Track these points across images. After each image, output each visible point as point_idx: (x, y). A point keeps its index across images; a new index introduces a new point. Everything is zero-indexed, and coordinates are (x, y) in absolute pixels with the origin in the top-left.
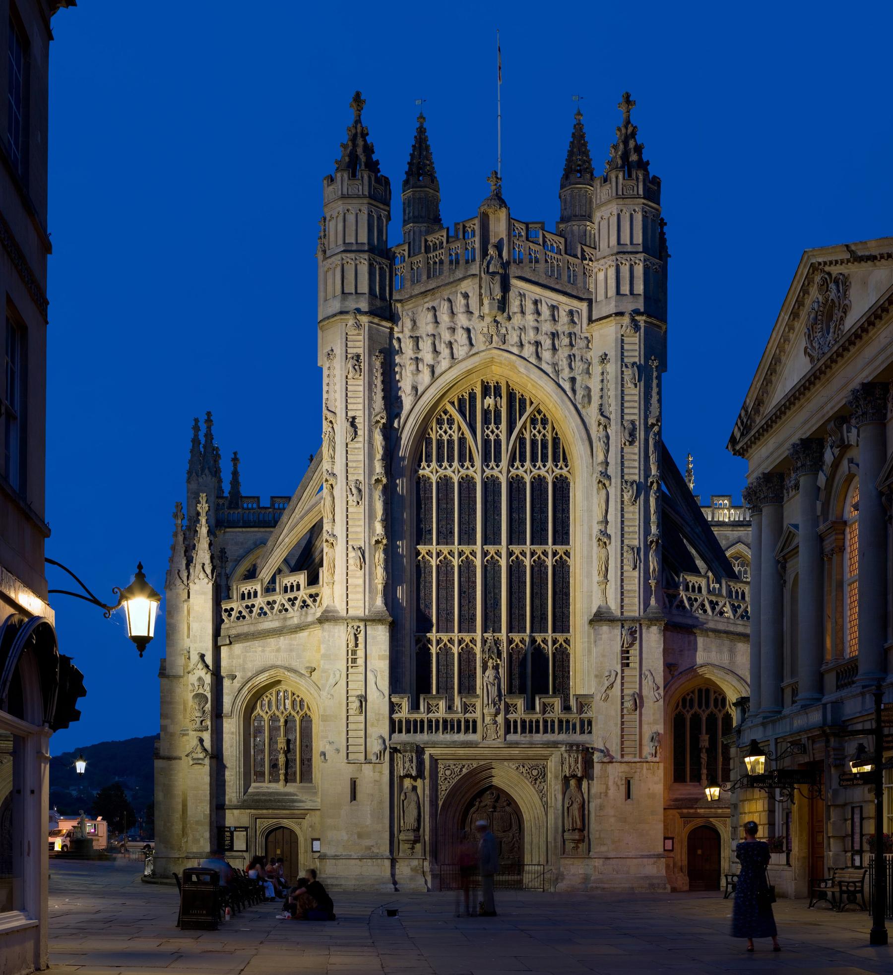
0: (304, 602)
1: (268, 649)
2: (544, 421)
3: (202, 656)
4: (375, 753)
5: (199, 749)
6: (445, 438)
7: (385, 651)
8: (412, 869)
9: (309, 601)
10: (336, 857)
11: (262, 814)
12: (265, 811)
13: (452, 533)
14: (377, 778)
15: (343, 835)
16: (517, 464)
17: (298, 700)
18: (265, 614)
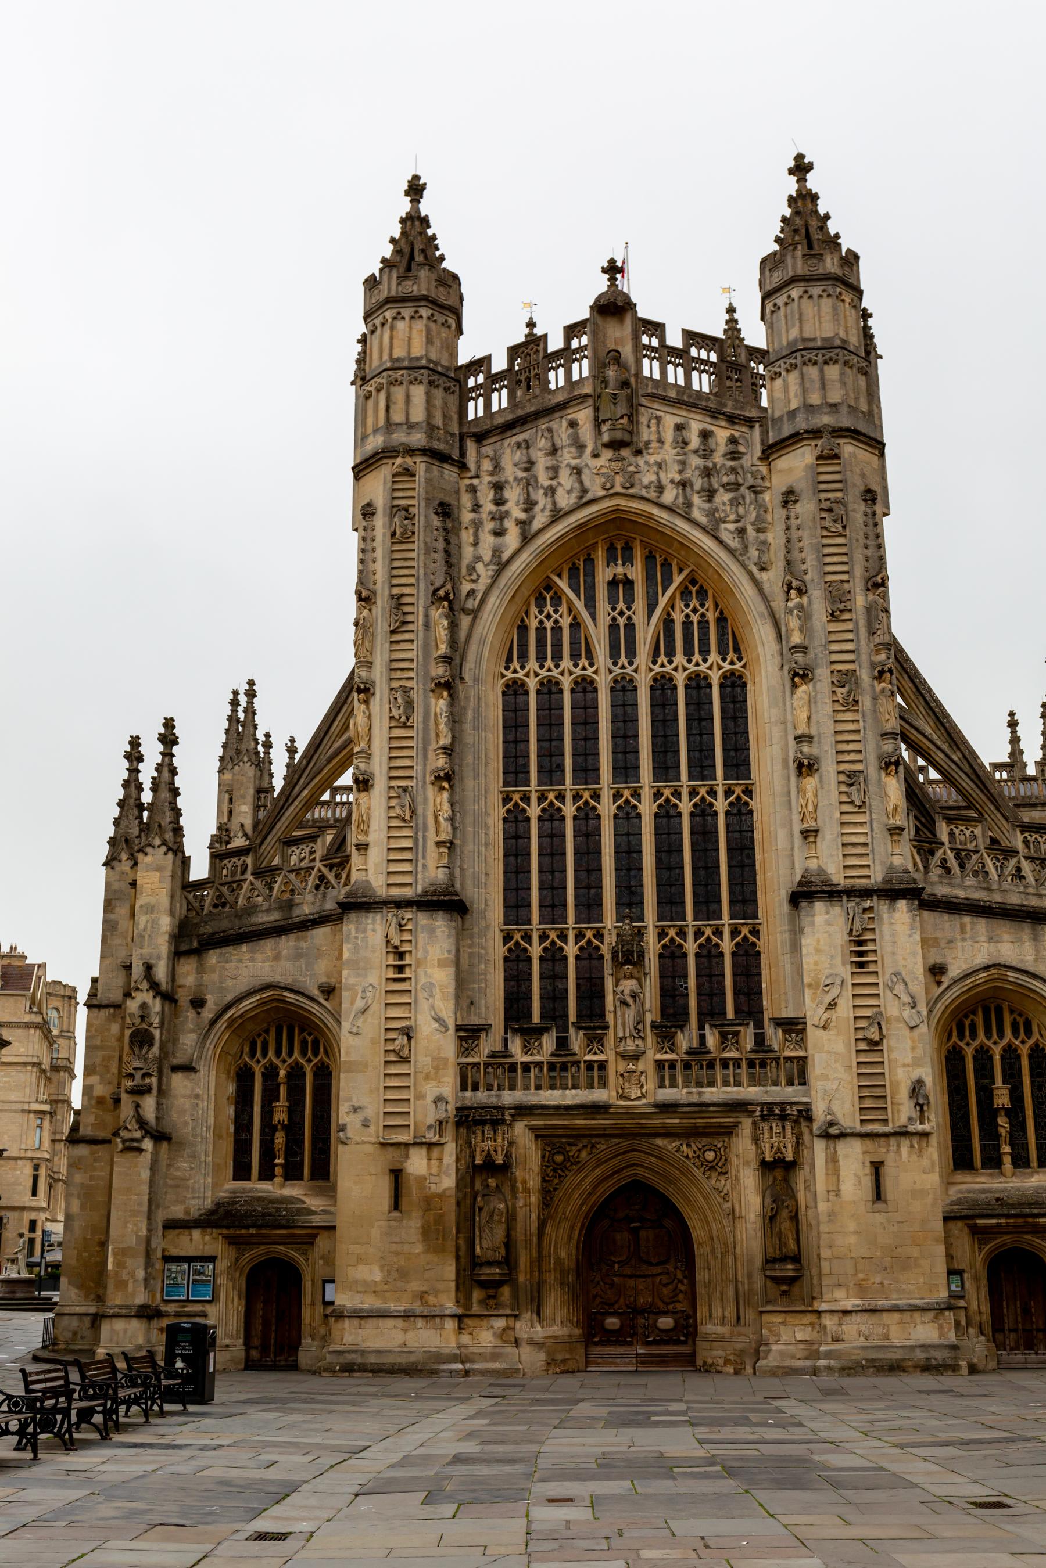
0: (322, 877)
1: (259, 956)
2: (702, 594)
3: (148, 968)
4: (430, 1127)
5: (133, 1125)
7: (449, 952)
8: (494, 1334)
9: (331, 877)
10: (361, 1316)
11: (241, 1236)
12: (243, 1231)
13: (561, 768)
15: (374, 1274)
16: (662, 658)
17: (310, 1039)
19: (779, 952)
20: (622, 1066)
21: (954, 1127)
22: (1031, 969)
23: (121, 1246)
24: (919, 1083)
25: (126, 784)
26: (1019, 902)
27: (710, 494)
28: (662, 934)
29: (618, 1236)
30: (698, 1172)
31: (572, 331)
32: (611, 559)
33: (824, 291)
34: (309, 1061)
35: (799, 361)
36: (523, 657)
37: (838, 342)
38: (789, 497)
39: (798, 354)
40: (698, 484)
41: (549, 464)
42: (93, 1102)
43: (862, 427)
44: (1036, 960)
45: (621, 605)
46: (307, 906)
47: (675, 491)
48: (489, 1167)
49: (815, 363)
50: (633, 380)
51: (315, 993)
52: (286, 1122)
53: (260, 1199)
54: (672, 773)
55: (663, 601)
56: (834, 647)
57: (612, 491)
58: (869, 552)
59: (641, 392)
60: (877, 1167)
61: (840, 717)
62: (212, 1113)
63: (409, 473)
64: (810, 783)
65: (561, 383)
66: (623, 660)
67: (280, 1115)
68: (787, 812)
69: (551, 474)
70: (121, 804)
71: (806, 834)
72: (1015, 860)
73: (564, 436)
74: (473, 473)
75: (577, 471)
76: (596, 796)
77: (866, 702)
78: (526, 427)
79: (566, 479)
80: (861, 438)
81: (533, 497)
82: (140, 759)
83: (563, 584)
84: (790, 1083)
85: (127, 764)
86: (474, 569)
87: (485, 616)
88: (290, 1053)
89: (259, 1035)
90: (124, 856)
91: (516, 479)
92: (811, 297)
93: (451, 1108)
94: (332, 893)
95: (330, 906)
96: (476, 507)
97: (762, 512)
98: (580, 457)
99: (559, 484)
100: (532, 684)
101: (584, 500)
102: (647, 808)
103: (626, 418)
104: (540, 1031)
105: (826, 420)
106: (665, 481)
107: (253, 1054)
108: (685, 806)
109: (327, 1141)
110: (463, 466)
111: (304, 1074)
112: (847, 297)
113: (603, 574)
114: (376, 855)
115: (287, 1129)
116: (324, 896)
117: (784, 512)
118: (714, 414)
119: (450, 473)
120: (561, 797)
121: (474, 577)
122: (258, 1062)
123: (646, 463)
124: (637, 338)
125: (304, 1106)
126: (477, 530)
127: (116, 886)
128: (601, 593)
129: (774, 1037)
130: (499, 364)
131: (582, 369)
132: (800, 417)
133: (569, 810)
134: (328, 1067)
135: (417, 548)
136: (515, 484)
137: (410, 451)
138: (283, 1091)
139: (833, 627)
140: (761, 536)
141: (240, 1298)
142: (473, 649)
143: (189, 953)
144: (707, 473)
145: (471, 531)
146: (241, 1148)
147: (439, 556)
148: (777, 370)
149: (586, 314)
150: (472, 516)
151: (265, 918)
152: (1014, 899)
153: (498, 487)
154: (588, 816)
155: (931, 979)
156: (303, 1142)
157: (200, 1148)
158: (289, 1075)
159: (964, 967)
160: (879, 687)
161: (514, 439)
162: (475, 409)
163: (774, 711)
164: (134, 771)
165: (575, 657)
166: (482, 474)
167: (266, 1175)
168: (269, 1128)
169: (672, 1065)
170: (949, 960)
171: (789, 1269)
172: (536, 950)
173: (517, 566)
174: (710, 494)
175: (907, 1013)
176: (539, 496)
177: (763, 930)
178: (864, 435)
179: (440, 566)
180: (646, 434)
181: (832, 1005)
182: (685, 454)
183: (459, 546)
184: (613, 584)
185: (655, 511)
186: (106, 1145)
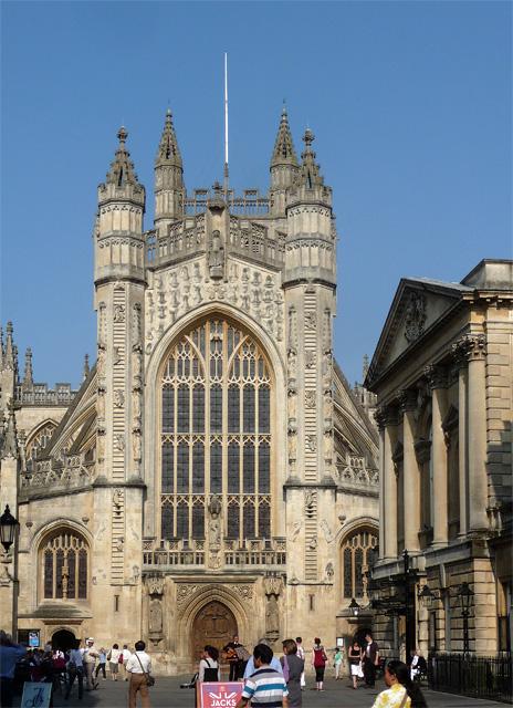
2: (253, 347)
16: (234, 377)
18: (54, 480)
20: (211, 555)
21: (345, 581)
24: (330, 565)
27: (258, 303)
28: (229, 498)
30: (240, 598)
32: (213, 329)
36: (172, 372)
37: (318, 236)
40: (253, 298)
43: (326, 278)
45: (216, 351)
46: (76, 484)
48: (155, 596)
51: (81, 521)
54: (236, 429)
55: (235, 350)
56: (307, 380)
58: (325, 337)
60: (311, 597)
61: (307, 411)
63: (121, 289)
64: (294, 439)
66: (216, 377)
67: (65, 571)
71: (290, 461)
75: (198, 289)
76: (203, 438)
77: (319, 405)
79: (193, 293)
83: (190, 339)
84: (279, 563)
93: (140, 571)
100: (176, 386)
102: (225, 444)
104: (177, 540)
105: (309, 275)
106: (238, 296)
108: (241, 444)
110: (146, 285)
112: (324, 211)
113: (210, 336)
114: (108, 464)
115: (68, 577)
119: (140, 288)
120: (187, 437)
128: (208, 345)
129: (274, 545)
132: (299, 272)
133: (191, 443)
135: (124, 326)
137: (125, 279)
138: (66, 561)
139: (307, 371)
142: (150, 371)
143: (25, 503)
144: (256, 293)
146: (48, 584)
147: (136, 329)
151: (58, 487)
153: (162, 295)
154: (199, 446)
155: (339, 522)
160: (325, 398)
165: (195, 375)
168: (60, 577)
169: (231, 554)
171: (274, 636)
172: (175, 504)
175: (328, 536)
176: (180, 300)
177: (272, 498)
179: (136, 333)
180: (230, 273)
181: (298, 532)
184: (213, 341)
185: (233, 310)
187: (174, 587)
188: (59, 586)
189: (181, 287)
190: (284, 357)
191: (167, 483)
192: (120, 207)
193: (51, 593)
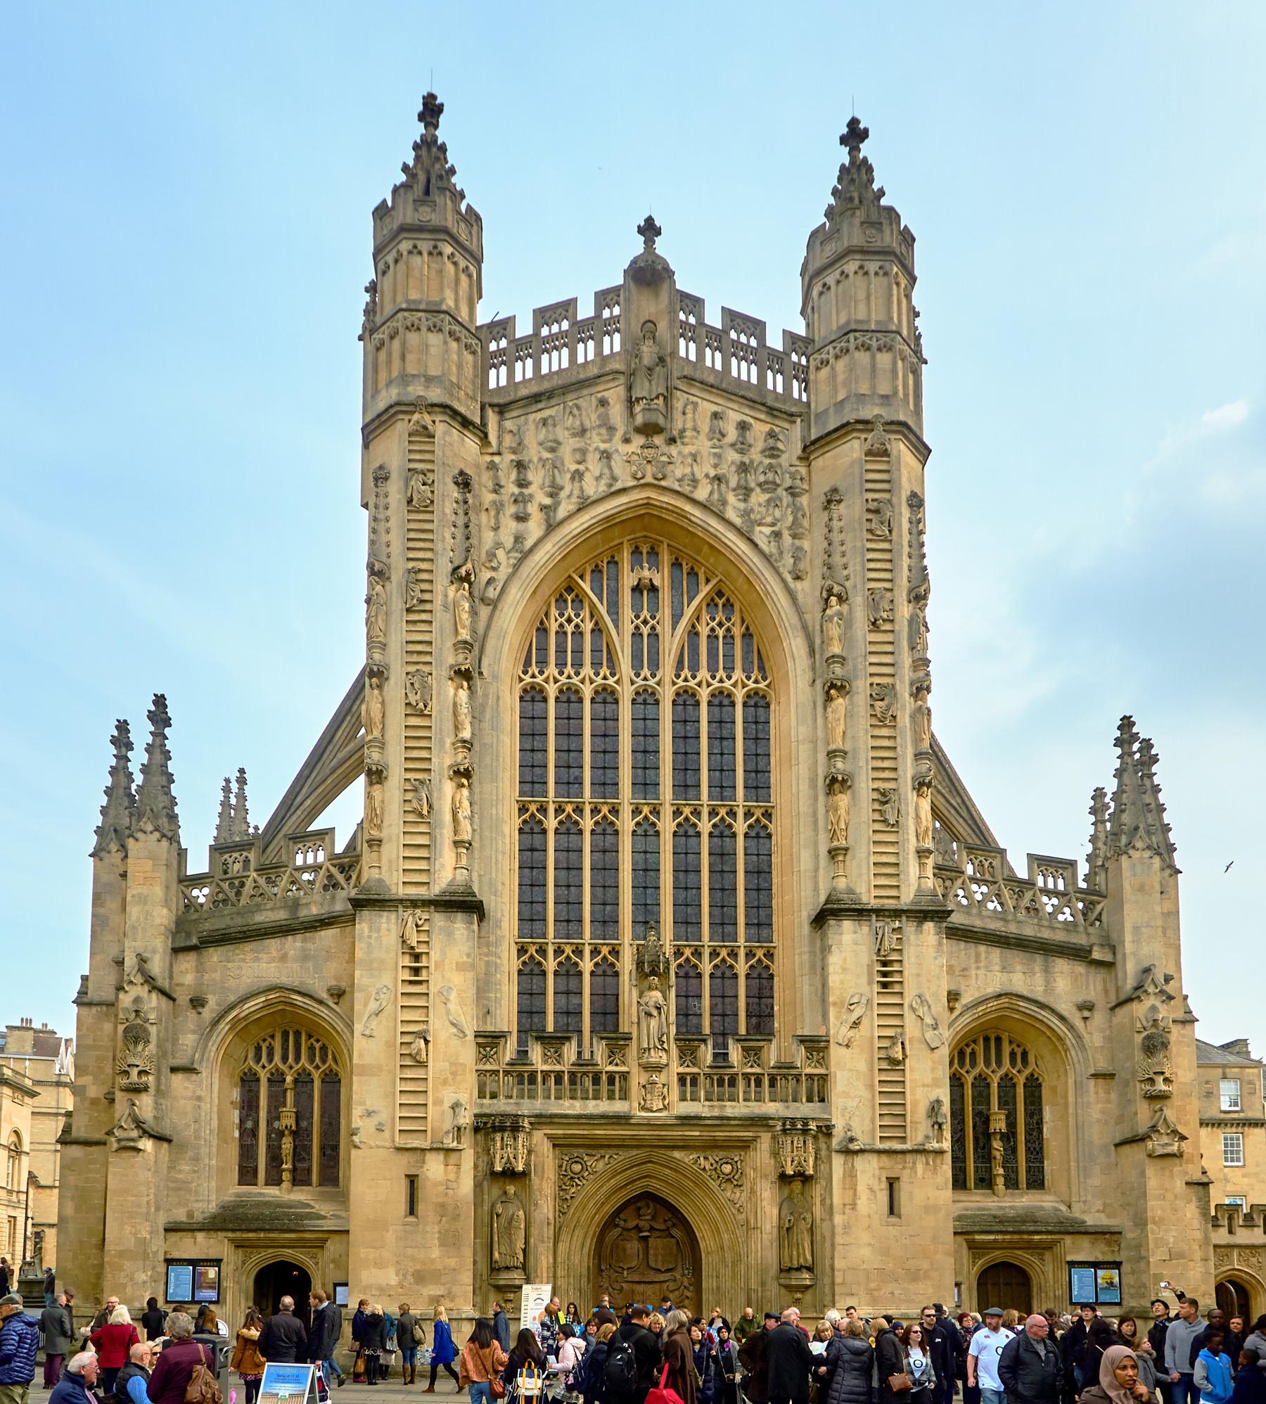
6: (570, 612)
14: (452, 1176)
17: (317, 1046)
19: (797, 973)
22: (1040, 999)
23: (119, 1248)
25: (113, 771)
26: (1032, 934)
27: (745, 492)
29: (628, 1245)
31: (604, 298)
33: (881, 268)
34: (317, 1067)
35: (852, 346)
38: (832, 499)
39: (851, 335)
41: (578, 446)
42: (87, 1104)
44: (1045, 991)
47: (709, 487)
49: (868, 349)
50: (668, 359)
52: (294, 1128)
53: (267, 1204)
57: (642, 481)
59: (676, 374)
62: (215, 1117)
65: (591, 356)
68: (812, 833)
69: (578, 457)
70: (108, 792)
72: (1031, 893)
73: (594, 417)
74: (494, 449)
75: (606, 456)
78: (553, 402)
79: (594, 466)
80: (911, 436)
81: (559, 481)
82: (130, 746)
85: (113, 750)
86: (495, 555)
87: (505, 609)
88: (297, 1058)
89: (264, 1040)
90: (114, 847)
91: (540, 459)
92: (866, 273)
94: (342, 894)
95: (340, 906)
96: (498, 487)
97: (799, 515)
98: (610, 440)
99: (587, 469)
101: (613, 489)
103: (661, 398)
107: (258, 1058)
109: (336, 1148)
110: (484, 438)
111: (312, 1081)
115: (295, 1134)
116: (333, 898)
117: (825, 516)
118: (753, 403)
119: (471, 444)
121: (494, 564)
122: (264, 1067)
123: (680, 453)
124: (673, 313)
125: (312, 1112)
126: (498, 513)
127: (105, 878)
130: (524, 328)
131: (613, 344)
132: (848, 407)
134: (337, 1075)
136: (540, 466)
138: (290, 1096)
140: (796, 541)
141: (247, 1299)
144: (743, 468)
145: (493, 513)
148: (824, 356)
149: (619, 280)
150: (492, 497)
152: (1029, 931)
153: (520, 466)
156: (311, 1147)
157: (204, 1151)
158: (296, 1081)
159: (977, 995)
161: (539, 415)
162: (497, 378)
163: (802, 729)
164: (122, 759)
166: (503, 450)
167: (274, 1179)
170: (963, 988)
173: (540, 556)
174: (745, 492)
176: (564, 480)
178: (915, 434)
182: (721, 447)
183: (479, 526)
185: (688, 508)
186: (101, 1148)
187: (545, 1148)
188: (275, 1159)
189: (566, 451)
190: (813, 616)
191: (531, 917)
192: (425, 246)
193: (255, 1171)
